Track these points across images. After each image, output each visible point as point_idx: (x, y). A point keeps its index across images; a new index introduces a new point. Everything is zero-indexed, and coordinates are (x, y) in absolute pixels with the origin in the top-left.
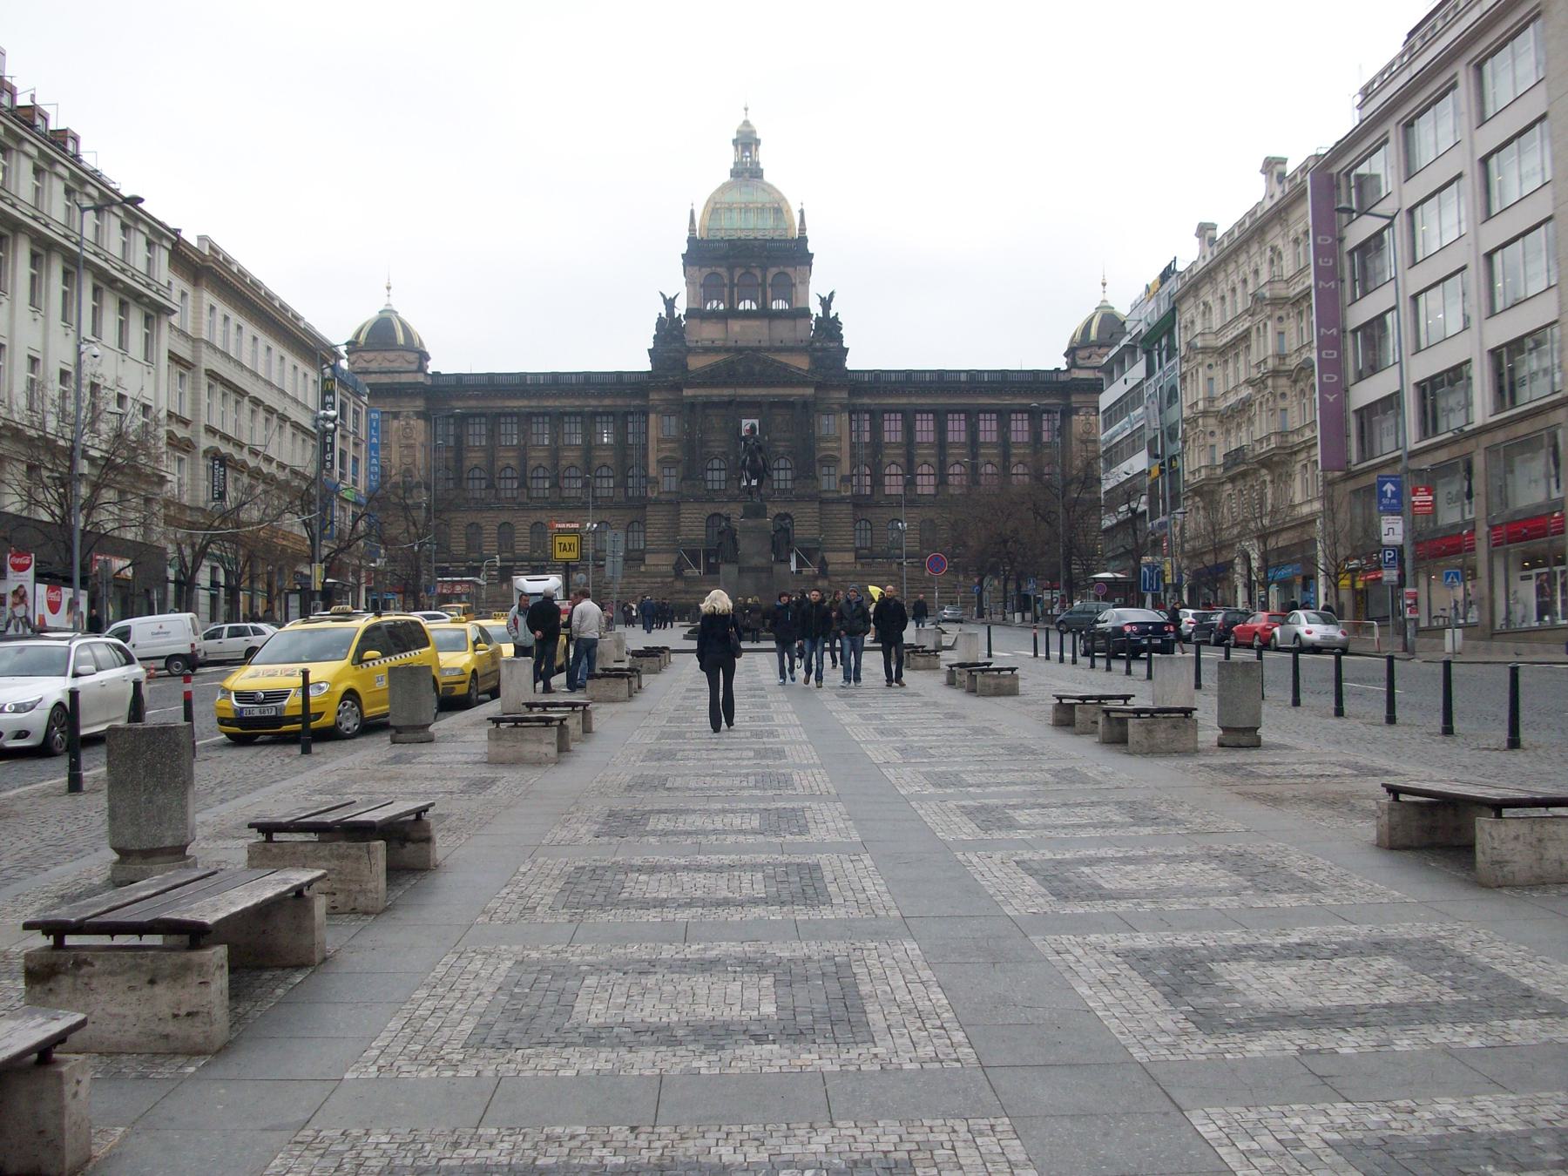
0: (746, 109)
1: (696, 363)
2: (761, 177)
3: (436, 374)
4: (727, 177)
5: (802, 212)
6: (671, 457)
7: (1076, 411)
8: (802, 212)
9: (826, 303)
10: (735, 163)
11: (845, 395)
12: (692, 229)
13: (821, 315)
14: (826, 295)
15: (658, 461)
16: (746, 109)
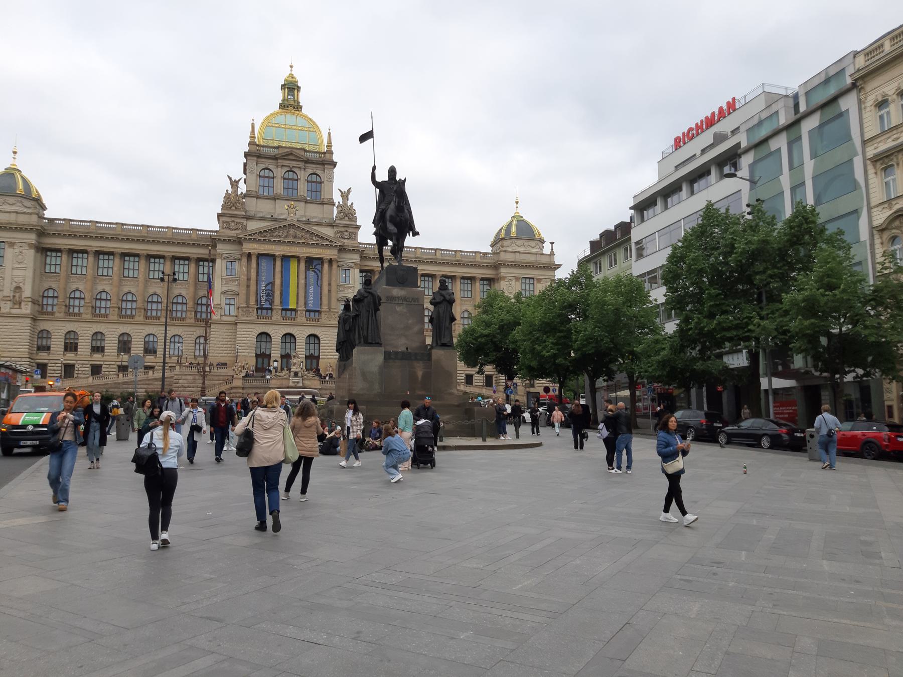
0: (291, 67)
1: (253, 226)
2: (301, 111)
3: (51, 220)
4: (276, 108)
5: (329, 134)
6: (230, 291)
7: (504, 278)
8: (329, 134)
9: (345, 195)
10: (283, 100)
11: (357, 256)
12: (252, 137)
13: (341, 203)
14: (345, 189)
15: (221, 293)
16: (291, 67)
